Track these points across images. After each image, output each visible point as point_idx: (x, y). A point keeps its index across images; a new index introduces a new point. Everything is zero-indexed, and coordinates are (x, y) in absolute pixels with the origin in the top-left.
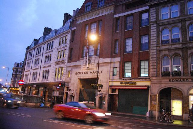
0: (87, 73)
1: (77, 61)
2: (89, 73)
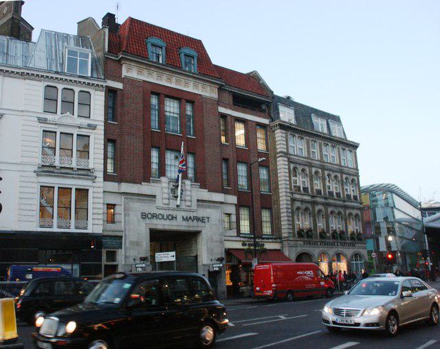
0: (174, 218)
1: (141, 184)
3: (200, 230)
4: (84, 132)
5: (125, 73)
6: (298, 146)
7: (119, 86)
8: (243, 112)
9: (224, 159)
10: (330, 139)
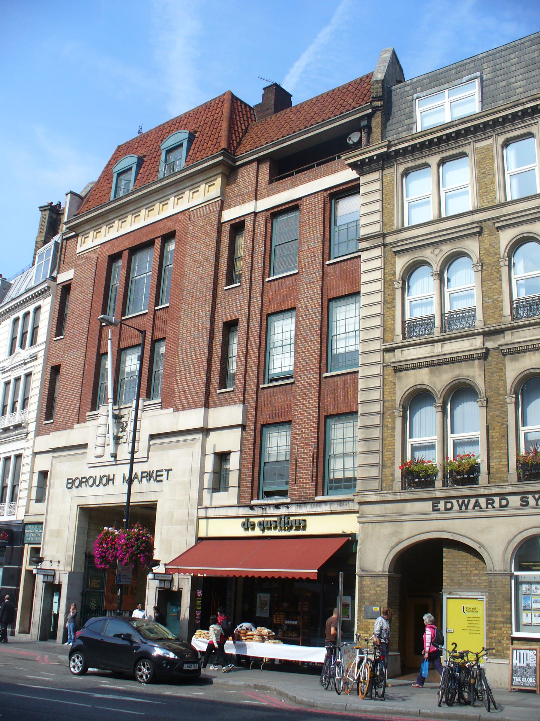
1: (72, 428)
3: (151, 498)
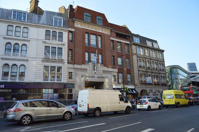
0: (93, 77)
2: (96, 77)
4: (60, 46)
5: (75, 26)
6: (141, 52)
7: (73, 30)
8: (120, 40)
9: (113, 56)
10: (153, 49)
